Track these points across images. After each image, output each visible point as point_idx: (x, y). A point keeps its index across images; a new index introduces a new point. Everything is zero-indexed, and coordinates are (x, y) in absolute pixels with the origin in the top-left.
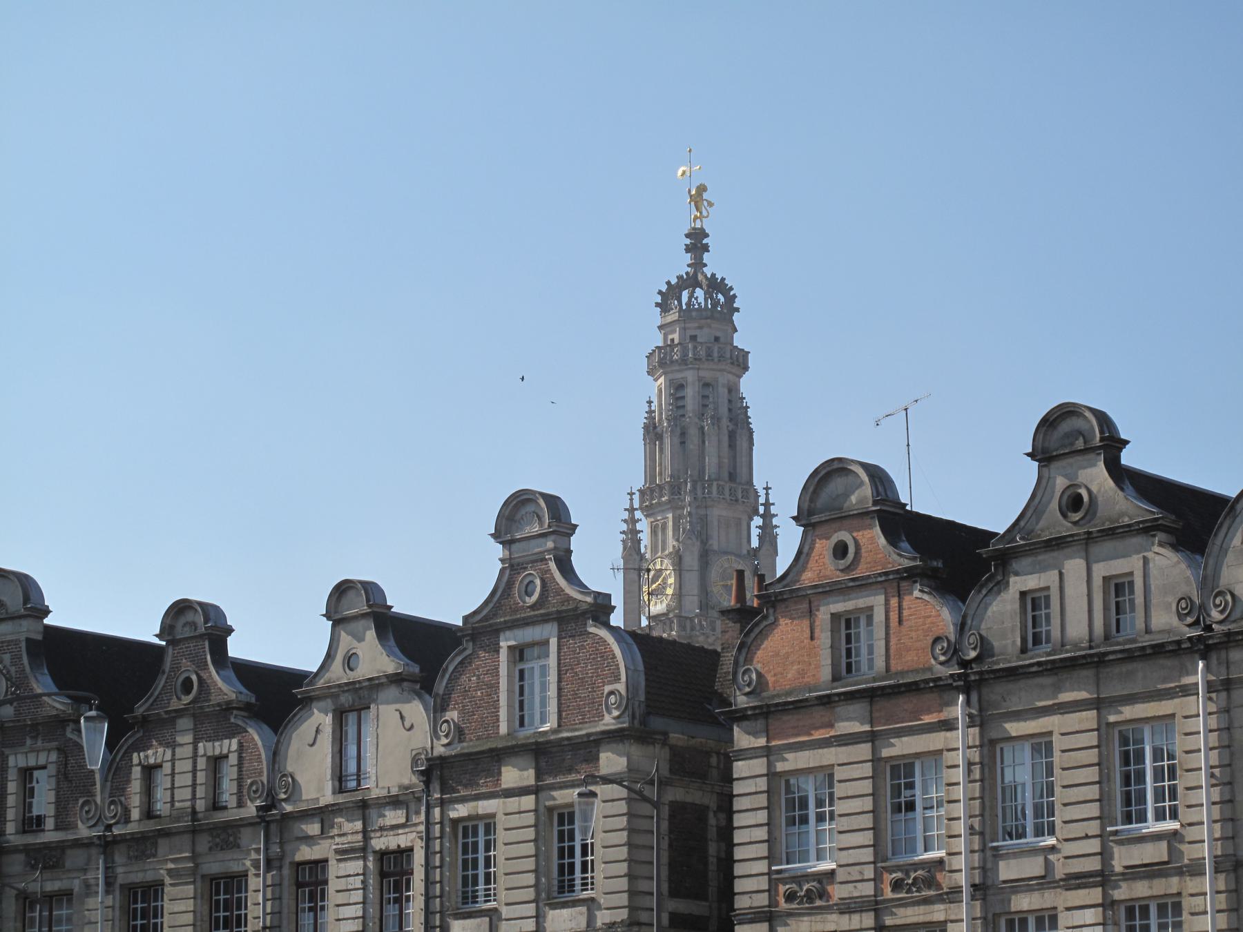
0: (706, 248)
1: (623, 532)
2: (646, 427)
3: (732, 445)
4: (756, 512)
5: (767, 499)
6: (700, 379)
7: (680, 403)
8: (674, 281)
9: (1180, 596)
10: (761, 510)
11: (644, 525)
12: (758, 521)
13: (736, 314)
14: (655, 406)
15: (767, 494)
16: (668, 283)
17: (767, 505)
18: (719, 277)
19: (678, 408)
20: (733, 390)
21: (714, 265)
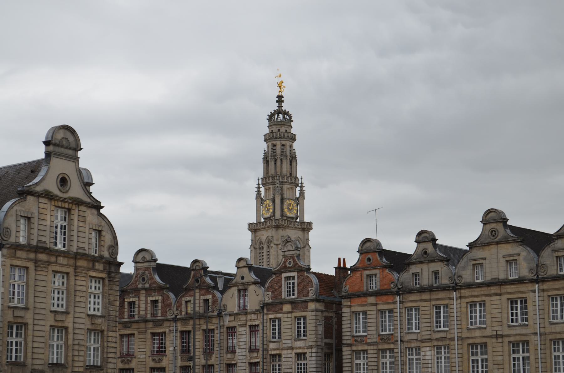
0: (283, 101)
1: (256, 191)
2: (263, 158)
3: (291, 164)
4: (298, 185)
5: (302, 181)
6: (281, 143)
7: (274, 151)
8: (273, 112)
9: (450, 276)
10: (300, 185)
11: (262, 189)
12: (298, 188)
13: (292, 122)
15: (302, 180)
16: (271, 112)
17: (302, 183)
18: (287, 111)
19: (274, 152)
20: (291, 146)
21: (285, 107)
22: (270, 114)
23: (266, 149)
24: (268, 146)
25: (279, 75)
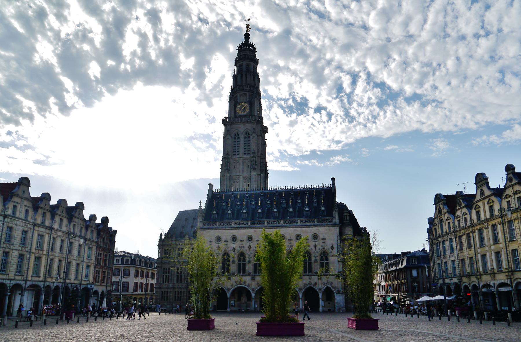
14: (236, 72)
21: (251, 40)
22: (239, 46)
23: (236, 70)
25: (248, 19)
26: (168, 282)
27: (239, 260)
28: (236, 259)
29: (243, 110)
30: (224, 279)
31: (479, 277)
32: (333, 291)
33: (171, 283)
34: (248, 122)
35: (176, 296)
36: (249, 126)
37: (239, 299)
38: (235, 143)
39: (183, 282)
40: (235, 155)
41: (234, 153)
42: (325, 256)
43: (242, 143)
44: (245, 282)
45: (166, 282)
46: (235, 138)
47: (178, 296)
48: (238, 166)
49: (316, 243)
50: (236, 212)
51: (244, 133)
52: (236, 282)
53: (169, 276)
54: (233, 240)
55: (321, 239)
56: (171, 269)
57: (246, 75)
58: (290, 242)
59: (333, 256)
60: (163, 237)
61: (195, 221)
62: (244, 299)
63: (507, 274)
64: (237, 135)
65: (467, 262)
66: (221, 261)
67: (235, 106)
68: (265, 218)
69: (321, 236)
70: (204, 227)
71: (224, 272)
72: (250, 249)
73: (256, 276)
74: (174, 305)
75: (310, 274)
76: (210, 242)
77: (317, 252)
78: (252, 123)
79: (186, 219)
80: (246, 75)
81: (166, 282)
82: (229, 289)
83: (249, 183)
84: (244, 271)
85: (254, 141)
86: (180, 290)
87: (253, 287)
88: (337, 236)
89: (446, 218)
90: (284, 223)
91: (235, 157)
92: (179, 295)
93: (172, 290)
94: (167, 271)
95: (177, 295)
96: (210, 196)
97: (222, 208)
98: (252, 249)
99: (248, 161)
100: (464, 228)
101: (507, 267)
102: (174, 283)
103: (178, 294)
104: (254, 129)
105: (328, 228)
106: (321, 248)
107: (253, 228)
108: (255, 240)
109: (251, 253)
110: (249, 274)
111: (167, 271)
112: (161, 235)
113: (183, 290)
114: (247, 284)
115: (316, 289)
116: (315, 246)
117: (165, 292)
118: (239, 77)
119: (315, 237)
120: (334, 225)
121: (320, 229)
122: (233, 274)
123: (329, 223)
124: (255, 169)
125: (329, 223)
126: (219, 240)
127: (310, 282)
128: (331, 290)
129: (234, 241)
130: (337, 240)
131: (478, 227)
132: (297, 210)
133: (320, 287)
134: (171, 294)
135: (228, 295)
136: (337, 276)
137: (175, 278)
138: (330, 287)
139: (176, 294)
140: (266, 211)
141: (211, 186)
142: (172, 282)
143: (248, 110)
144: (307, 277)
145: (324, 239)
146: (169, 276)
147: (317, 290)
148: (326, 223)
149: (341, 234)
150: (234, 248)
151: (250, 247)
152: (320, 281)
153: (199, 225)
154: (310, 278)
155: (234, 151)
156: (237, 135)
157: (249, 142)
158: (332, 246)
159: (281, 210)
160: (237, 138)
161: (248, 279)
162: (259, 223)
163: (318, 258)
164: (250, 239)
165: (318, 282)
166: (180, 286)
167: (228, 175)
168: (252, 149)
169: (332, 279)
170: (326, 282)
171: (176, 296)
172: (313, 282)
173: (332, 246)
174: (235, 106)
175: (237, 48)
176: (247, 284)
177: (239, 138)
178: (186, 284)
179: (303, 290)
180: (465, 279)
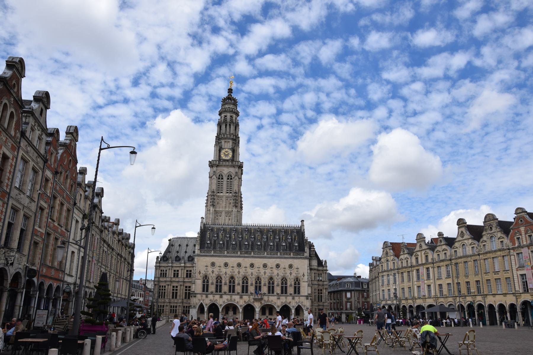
8: (225, 97)
20: (236, 119)
22: (223, 98)
24: (221, 118)
26: (164, 298)
27: (230, 282)
28: (228, 282)
29: (227, 155)
30: (217, 297)
31: (414, 300)
32: (302, 309)
33: (167, 299)
34: (231, 166)
35: (171, 310)
36: (233, 170)
37: (227, 313)
38: (219, 183)
39: (178, 298)
40: (219, 192)
41: (218, 191)
42: (297, 281)
43: (225, 183)
44: (235, 300)
45: (162, 297)
46: (219, 178)
47: (173, 310)
48: (221, 203)
49: (291, 271)
50: (226, 242)
51: (227, 175)
52: (227, 300)
53: (165, 292)
54: (225, 266)
55: (295, 268)
56: (167, 286)
57: (230, 125)
58: (271, 270)
59: (304, 282)
60: (159, 260)
61: (188, 247)
62: (231, 313)
63: (434, 299)
64: (221, 176)
65: (406, 290)
66: (215, 283)
67: (220, 151)
68: (250, 249)
69: (295, 266)
70: (201, 254)
71: (216, 291)
72: (239, 274)
73: (244, 295)
74: (170, 316)
75: (286, 295)
76: (207, 266)
77: (292, 278)
78: (235, 167)
79: (180, 245)
80: (230, 125)
81: (162, 297)
82: (221, 305)
83: (230, 218)
84: (234, 291)
85: (235, 182)
86: (175, 305)
87: (241, 304)
88: (308, 267)
89: (392, 259)
90: (267, 254)
91: (218, 194)
92: (175, 309)
93: (168, 304)
94: (164, 288)
95: (172, 309)
96: (202, 227)
97: (214, 238)
98: (240, 274)
99: (230, 199)
100: (405, 268)
101: (435, 295)
102: (170, 299)
103: (174, 307)
104: (236, 173)
105: (300, 260)
106: (295, 275)
107: (242, 257)
108: (243, 267)
109: (240, 277)
110: (238, 294)
111: (164, 288)
112: (158, 257)
113: (178, 305)
114: (236, 301)
115: (290, 306)
116: (291, 274)
117: (161, 306)
118: (223, 127)
119: (291, 267)
120: (306, 258)
121: (295, 260)
122: (225, 293)
123: (302, 256)
124: (236, 207)
125: (302, 256)
126: (213, 265)
127: (286, 301)
128: (301, 307)
129: (226, 267)
130: (308, 270)
131: (416, 268)
132: (275, 244)
133: (293, 305)
134: (168, 308)
135: (220, 310)
136: (307, 297)
137: (171, 295)
138: (301, 305)
139: (171, 307)
140: (251, 243)
141: (202, 219)
142: (168, 298)
143: (231, 156)
144: (284, 297)
145: (298, 268)
146: (165, 292)
147: (291, 307)
148: (299, 256)
149: (310, 265)
150: (226, 272)
151: (239, 272)
152: (293, 301)
153: (197, 252)
154: (286, 298)
155: (219, 189)
156: (221, 176)
157: (231, 183)
158: (304, 274)
159: (263, 243)
160: (221, 178)
161: (236, 298)
162: (246, 253)
163: (293, 283)
164: (239, 265)
165: (291, 301)
166: (176, 301)
167: (214, 210)
168: (235, 190)
169: (303, 299)
170: (298, 302)
171: (171, 310)
172: (288, 301)
173: (304, 274)
174: (220, 151)
175: (222, 100)
176: (236, 301)
177: (222, 179)
178: (182, 300)
179: (281, 307)
180: (403, 302)
